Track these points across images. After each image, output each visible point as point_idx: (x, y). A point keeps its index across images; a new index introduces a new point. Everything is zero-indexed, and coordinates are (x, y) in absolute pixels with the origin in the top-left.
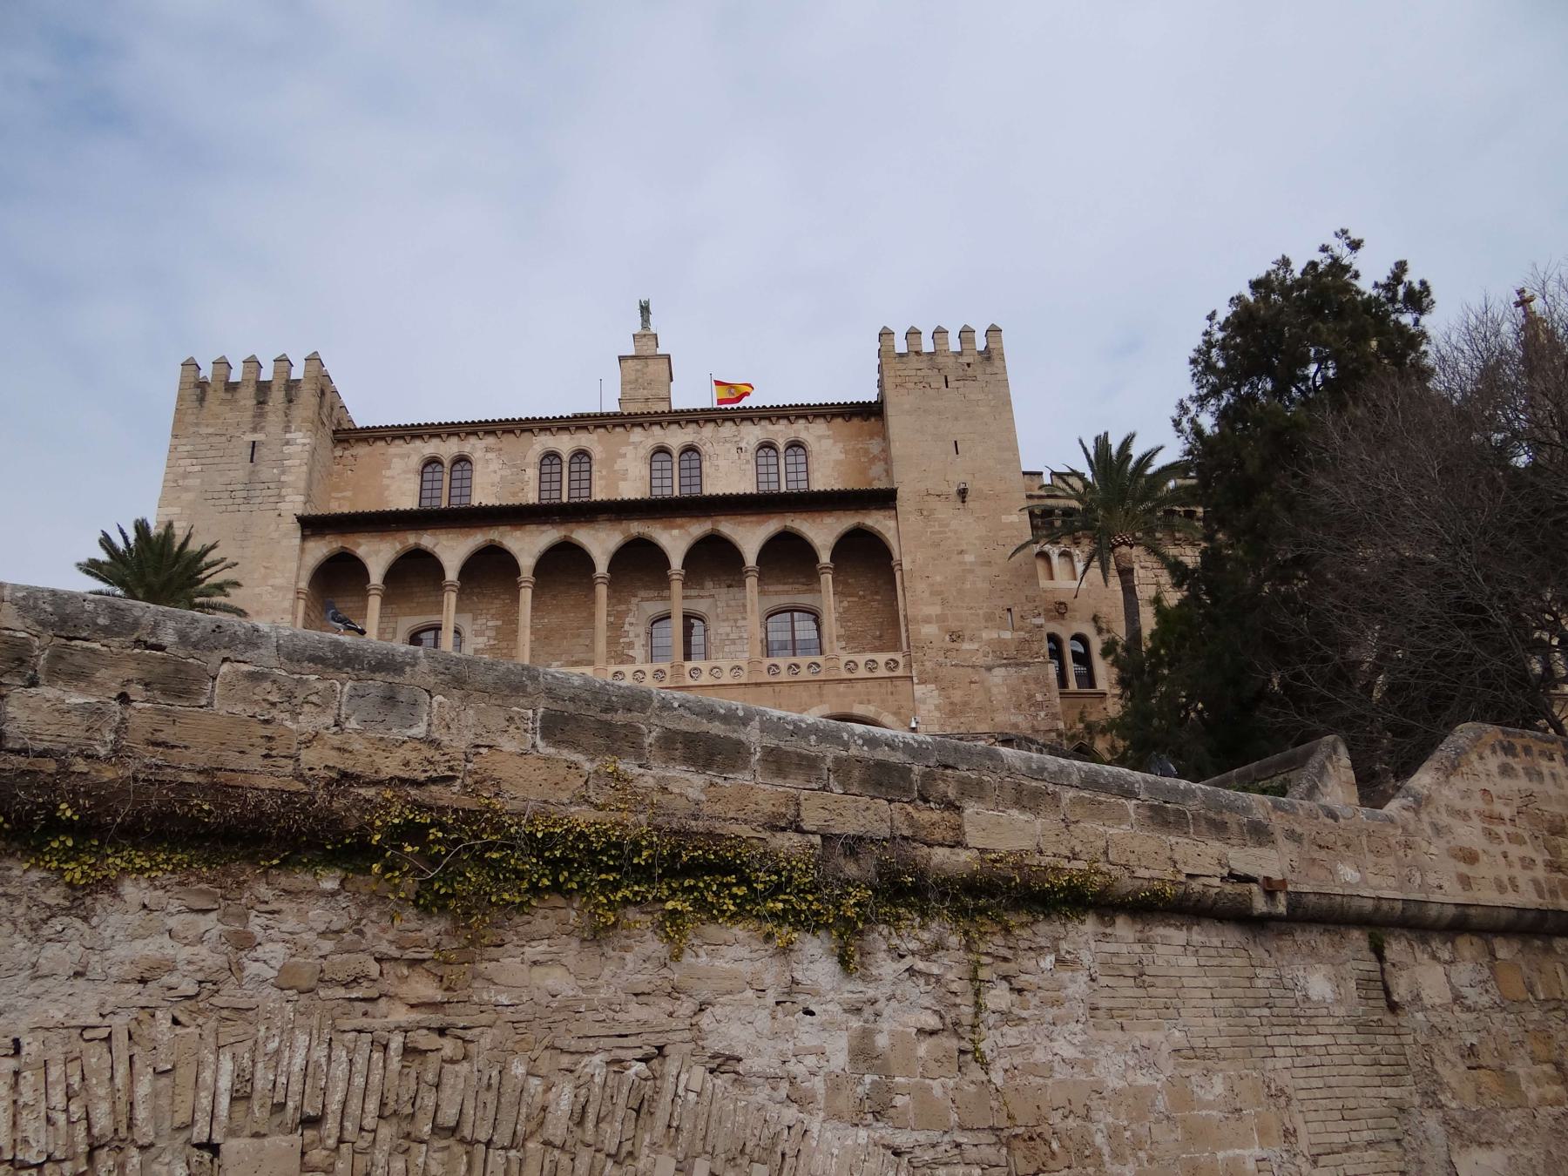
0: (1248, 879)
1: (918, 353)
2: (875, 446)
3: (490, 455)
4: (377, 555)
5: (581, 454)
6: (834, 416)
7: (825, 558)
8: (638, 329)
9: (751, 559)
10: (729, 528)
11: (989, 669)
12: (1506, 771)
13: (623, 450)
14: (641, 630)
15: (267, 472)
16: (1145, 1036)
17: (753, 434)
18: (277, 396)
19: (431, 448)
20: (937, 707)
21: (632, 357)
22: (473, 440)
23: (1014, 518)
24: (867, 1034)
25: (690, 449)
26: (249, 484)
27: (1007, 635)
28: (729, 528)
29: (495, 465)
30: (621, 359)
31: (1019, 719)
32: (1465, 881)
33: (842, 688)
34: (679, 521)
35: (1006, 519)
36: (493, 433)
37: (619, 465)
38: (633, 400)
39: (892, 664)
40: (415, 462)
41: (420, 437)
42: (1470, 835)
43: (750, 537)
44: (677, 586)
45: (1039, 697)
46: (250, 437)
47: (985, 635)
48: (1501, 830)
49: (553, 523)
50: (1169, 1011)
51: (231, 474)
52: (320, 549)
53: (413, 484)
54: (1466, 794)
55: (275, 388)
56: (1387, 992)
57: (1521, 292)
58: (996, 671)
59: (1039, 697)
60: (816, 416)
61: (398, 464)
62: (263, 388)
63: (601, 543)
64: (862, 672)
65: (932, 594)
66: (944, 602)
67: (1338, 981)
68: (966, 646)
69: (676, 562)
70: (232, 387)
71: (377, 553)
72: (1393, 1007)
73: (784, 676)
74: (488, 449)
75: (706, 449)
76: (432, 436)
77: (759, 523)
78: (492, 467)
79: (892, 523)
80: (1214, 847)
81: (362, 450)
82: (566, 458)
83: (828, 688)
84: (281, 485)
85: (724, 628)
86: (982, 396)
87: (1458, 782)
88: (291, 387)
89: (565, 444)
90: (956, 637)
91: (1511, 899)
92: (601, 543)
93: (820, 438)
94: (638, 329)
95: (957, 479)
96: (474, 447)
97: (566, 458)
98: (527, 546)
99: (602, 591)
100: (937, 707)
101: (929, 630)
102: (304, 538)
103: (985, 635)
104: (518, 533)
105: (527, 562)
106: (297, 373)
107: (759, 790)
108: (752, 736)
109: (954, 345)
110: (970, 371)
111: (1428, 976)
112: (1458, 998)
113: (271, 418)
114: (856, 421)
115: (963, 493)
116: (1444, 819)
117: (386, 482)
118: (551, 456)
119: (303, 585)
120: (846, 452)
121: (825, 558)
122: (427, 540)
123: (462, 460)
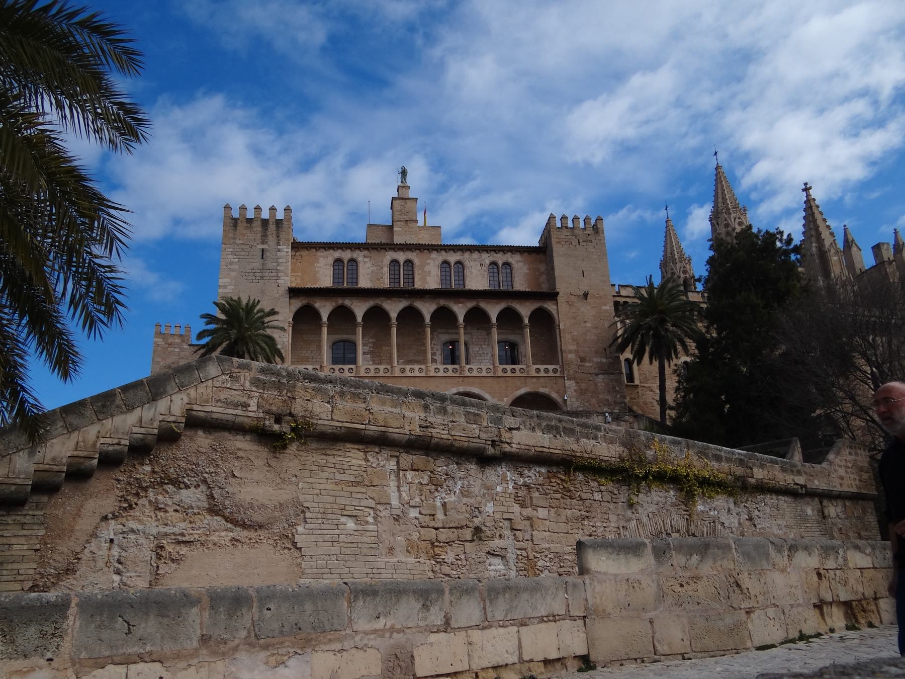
0: (798, 484)
1: (566, 228)
2: (542, 267)
3: (366, 260)
4: (325, 309)
5: (409, 262)
6: (524, 252)
7: (526, 321)
8: (400, 184)
9: (494, 320)
10: (483, 305)
11: (597, 375)
12: (850, 454)
13: (428, 261)
14: (439, 347)
15: (271, 265)
16: (780, 522)
17: (487, 258)
18: (272, 227)
19: (338, 254)
20: (575, 391)
21: (399, 198)
22: (358, 252)
23: (607, 308)
24: (739, 519)
25: (459, 263)
26: (263, 268)
27: (604, 360)
28: (483, 305)
29: (368, 265)
30: (393, 199)
31: (609, 397)
32: (841, 485)
33: (534, 380)
34: (461, 300)
35: (604, 308)
36: (367, 249)
37: (427, 268)
38: (399, 221)
39: (555, 371)
40: (331, 260)
41: (333, 248)
43: (493, 311)
44: (462, 331)
45: (617, 388)
46: (261, 247)
47: (595, 360)
48: (849, 470)
49: (405, 298)
50: (783, 516)
51: (254, 264)
53: (330, 272)
54: (841, 461)
55: (271, 223)
56: (823, 513)
57: (806, 184)
58: (600, 376)
59: (617, 388)
60: (516, 251)
62: (265, 222)
63: (427, 309)
64: (542, 374)
65: (573, 340)
66: (578, 344)
67: (813, 510)
68: (587, 364)
69: (461, 319)
70: (250, 221)
71: (325, 306)
72: (824, 517)
73: (509, 374)
74: (365, 257)
75: (467, 263)
76: (338, 248)
77: (498, 303)
78: (368, 265)
79: (555, 307)
80: (792, 477)
81: (304, 253)
82: (402, 263)
83: (528, 380)
84: (278, 271)
85: (476, 349)
86: (594, 250)
87: (839, 457)
88: (279, 223)
90: (583, 360)
91: (851, 490)
92: (427, 309)
93: (518, 262)
94: (400, 184)
95: (586, 288)
96: (359, 255)
97: (402, 263)
98: (394, 308)
100: (575, 391)
101: (571, 356)
102: (290, 298)
103: (595, 360)
104: (389, 301)
105: (394, 315)
106: (280, 215)
108: (722, 454)
109: (582, 225)
110: (589, 238)
111: (833, 510)
112: (838, 516)
113: (270, 238)
114: (533, 255)
115: (586, 296)
116: (837, 468)
117: (317, 269)
118: (395, 262)
119: (291, 320)
120: (529, 269)
121: (526, 321)
122: (347, 302)
123: (353, 261)
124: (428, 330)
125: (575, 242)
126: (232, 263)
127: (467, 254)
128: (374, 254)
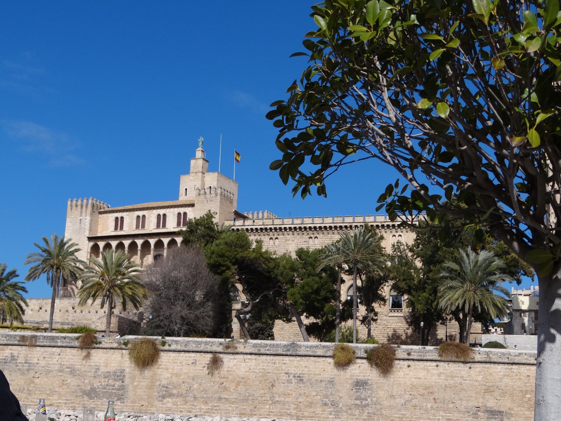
4: (101, 244)
15: (83, 226)
17: (177, 210)
18: (84, 208)
22: (124, 213)
26: (80, 228)
29: (128, 219)
37: (151, 219)
40: (114, 219)
42: (98, 324)
52: (92, 244)
53: (113, 224)
61: (110, 218)
81: (104, 215)
89: (141, 213)
96: (124, 214)
99: (139, 253)
107: (29, 324)
119: (89, 251)
124: (139, 253)
125: (205, 202)
126: (69, 227)
127: (168, 210)
128: (131, 213)
